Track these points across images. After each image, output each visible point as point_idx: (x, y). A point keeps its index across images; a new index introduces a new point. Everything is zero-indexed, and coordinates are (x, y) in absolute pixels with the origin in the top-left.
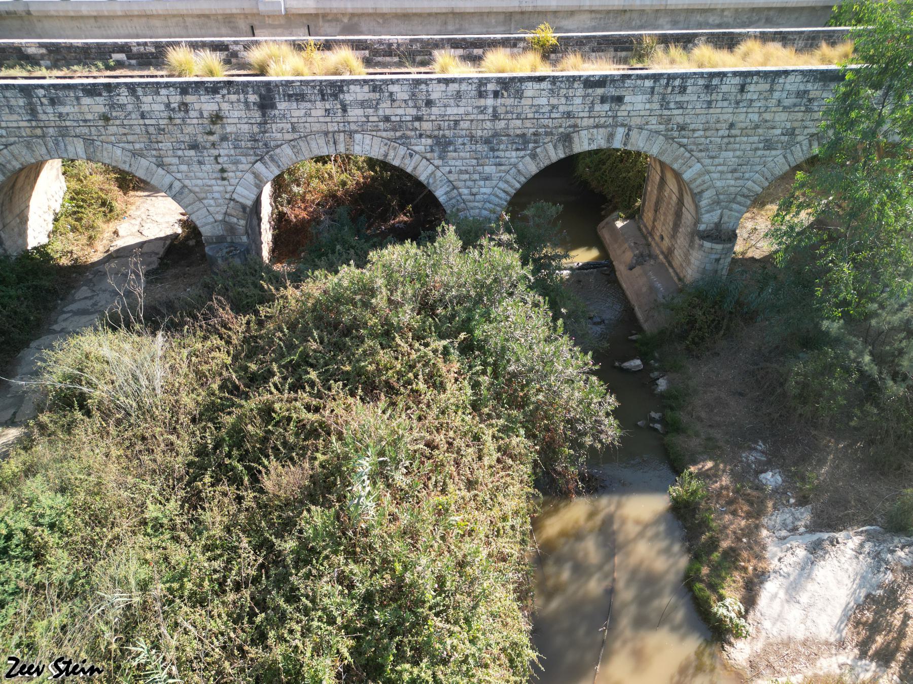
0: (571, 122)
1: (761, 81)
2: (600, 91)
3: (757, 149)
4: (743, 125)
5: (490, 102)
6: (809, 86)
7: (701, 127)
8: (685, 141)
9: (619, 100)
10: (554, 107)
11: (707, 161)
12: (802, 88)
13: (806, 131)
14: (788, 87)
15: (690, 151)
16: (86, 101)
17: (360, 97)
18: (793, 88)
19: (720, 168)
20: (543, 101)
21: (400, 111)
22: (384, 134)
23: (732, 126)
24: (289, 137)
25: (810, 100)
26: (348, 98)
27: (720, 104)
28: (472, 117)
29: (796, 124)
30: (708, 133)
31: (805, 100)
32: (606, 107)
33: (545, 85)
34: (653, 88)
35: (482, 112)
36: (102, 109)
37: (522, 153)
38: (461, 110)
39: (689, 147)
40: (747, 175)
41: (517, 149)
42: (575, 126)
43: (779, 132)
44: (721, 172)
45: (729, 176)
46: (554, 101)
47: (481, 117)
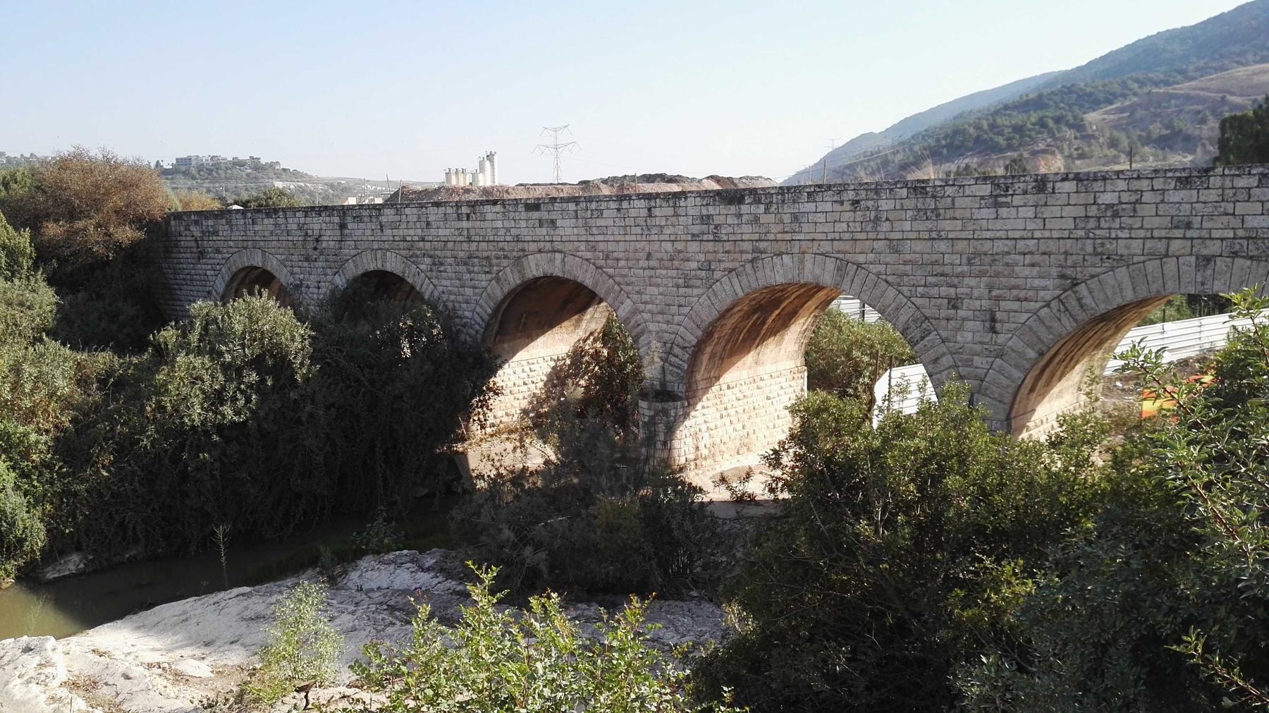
0: (520, 245)
1: (664, 204)
2: (536, 215)
3: (678, 287)
4: (659, 255)
5: (465, 224)
6: (711, 210)
7: (621, 255)
8: (611, 271)
9: (553, 222)
10: (508, 230)
11: (636, 297)
12: (704, 212)
13: (723, 266)
15: (619, 284)
16: (266, 221)
19: (649, 307)
20: (499, 224)
21: (412, 232)
22: (403, 252)
23: (649, 257)
26: (383, 219)
28: (454, 238)
29: (710, 257)
30: (631, 264)
31: (712, 227)
32: (544, 231)
33: (498, 208)
34: (576, 211)
35: (460, 235)
36: (271, 228)
37: (489, 276)
38: (447, 232)
39: (617, 279)
40: (677, 319)
41: (486, 273)
42: (523, 250)
43: (694, 265)
44: (652, 313)
45: (659, 318)
46: (507, 224)
47: (460, 238)
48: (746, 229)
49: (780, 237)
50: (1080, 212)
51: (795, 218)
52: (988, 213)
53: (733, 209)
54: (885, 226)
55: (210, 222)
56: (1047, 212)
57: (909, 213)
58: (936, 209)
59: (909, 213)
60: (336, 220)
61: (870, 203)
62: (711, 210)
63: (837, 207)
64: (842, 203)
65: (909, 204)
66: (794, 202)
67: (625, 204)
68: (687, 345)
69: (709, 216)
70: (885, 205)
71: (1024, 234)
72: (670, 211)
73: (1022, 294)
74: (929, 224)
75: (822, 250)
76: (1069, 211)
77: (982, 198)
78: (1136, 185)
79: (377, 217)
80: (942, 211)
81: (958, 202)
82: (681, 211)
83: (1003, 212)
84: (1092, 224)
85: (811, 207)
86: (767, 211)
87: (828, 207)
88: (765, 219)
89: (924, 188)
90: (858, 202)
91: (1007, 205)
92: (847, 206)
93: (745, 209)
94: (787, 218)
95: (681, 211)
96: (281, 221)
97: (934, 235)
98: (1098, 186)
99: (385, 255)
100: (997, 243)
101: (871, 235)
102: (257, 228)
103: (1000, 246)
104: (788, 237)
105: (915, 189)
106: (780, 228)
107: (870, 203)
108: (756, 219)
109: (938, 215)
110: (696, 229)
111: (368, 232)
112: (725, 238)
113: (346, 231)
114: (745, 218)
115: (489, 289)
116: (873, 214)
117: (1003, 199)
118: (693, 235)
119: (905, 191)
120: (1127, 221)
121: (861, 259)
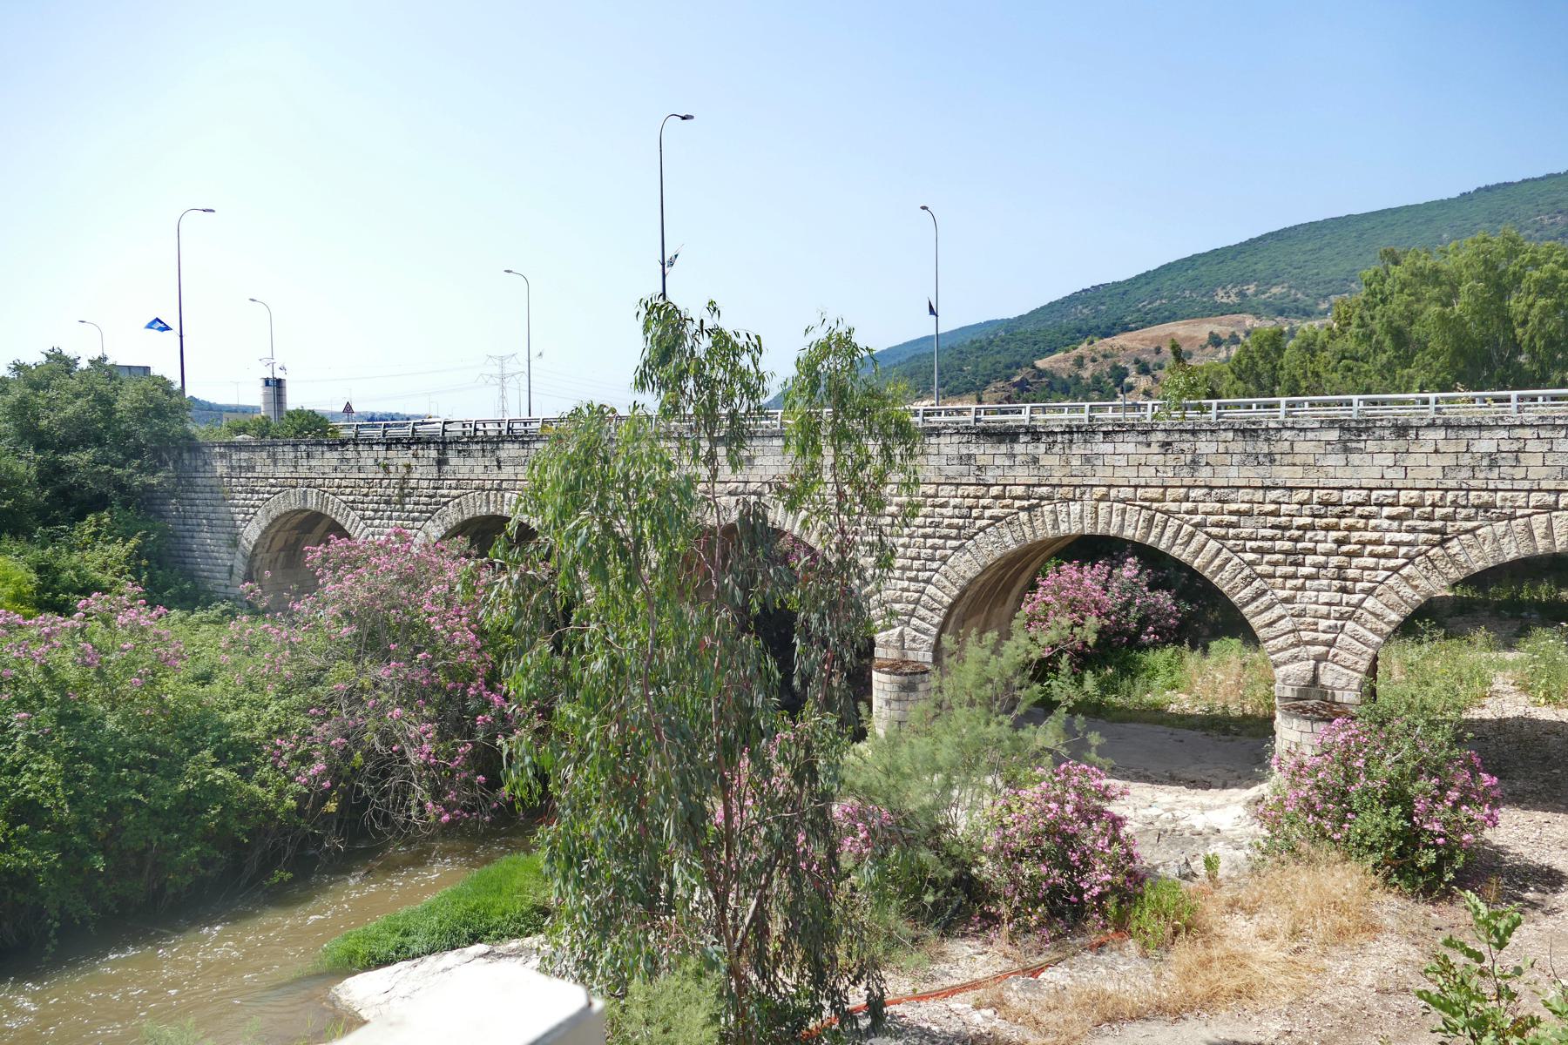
6: (973, 450)
12: (964, 451)
14: (946, 450)
16: (328, 455)
17: (513, 453)
18: (952, 451)
24: (454, 492)
25: (979, 468)
26: (502, 454)
36: (335, 463)
49: (1065, 481)
50: (1449, 460)
51: (1087, 459)
52: (1339, 459)
53: (1003, 448)
54: (1204, 474)
55: (244, 455)
56: (1410, 461)
57: (1236, 458)
58: (1270, 454)
59: (1236, 458)
60: (433, 454)
61: (1185, 446)
62: (973, 450)
63: (1145, 450)
64: (1149, 445)
65: (1238, 446)
66: (1086, 441)
68: (936, 605)
69: (969, 456)
71: (1382, 483)
73: (1379, 549)
74: (1261, 470)
75: (1122, 496)
76: (1435, 460)
77: (1328, 443)
78: (1519, 433)
79: (493, 451)
80: (1278, 457)
81: (1298, 447)
83: (1355, 458)
84: (1465, 473)
85: (1108, 448)
86: (1048, 451)
87: (1130, 448)
88: (1046, 460)
89: (1255, 431)
90: (1169, 444)
91: (1361, 451)
92: (1155, 448)
93: (1019, 448)
94: (1076, 462)
96: (349, 455)
97: (1268, 483)
98: (1474, 434)
100: (1346, 493)
101: (1188, 482)
102: (313, 463)
103: (1350, 496)
104: (1076, 481)
105: (1243, 431)
106: (1067, 470)
107: (1185, 446)
108: (1035, 460)
109: (1272, 461)
110: (952, 470)
111: (479, 470)
112: (992, 481)
113: (446, 468)
114: (1019, 459)
116: (1189, 457)
117: (1354, 445)
118: (947, 477)
119: (1230, 435)
120: (1506, 471)
121: (1173, 507)
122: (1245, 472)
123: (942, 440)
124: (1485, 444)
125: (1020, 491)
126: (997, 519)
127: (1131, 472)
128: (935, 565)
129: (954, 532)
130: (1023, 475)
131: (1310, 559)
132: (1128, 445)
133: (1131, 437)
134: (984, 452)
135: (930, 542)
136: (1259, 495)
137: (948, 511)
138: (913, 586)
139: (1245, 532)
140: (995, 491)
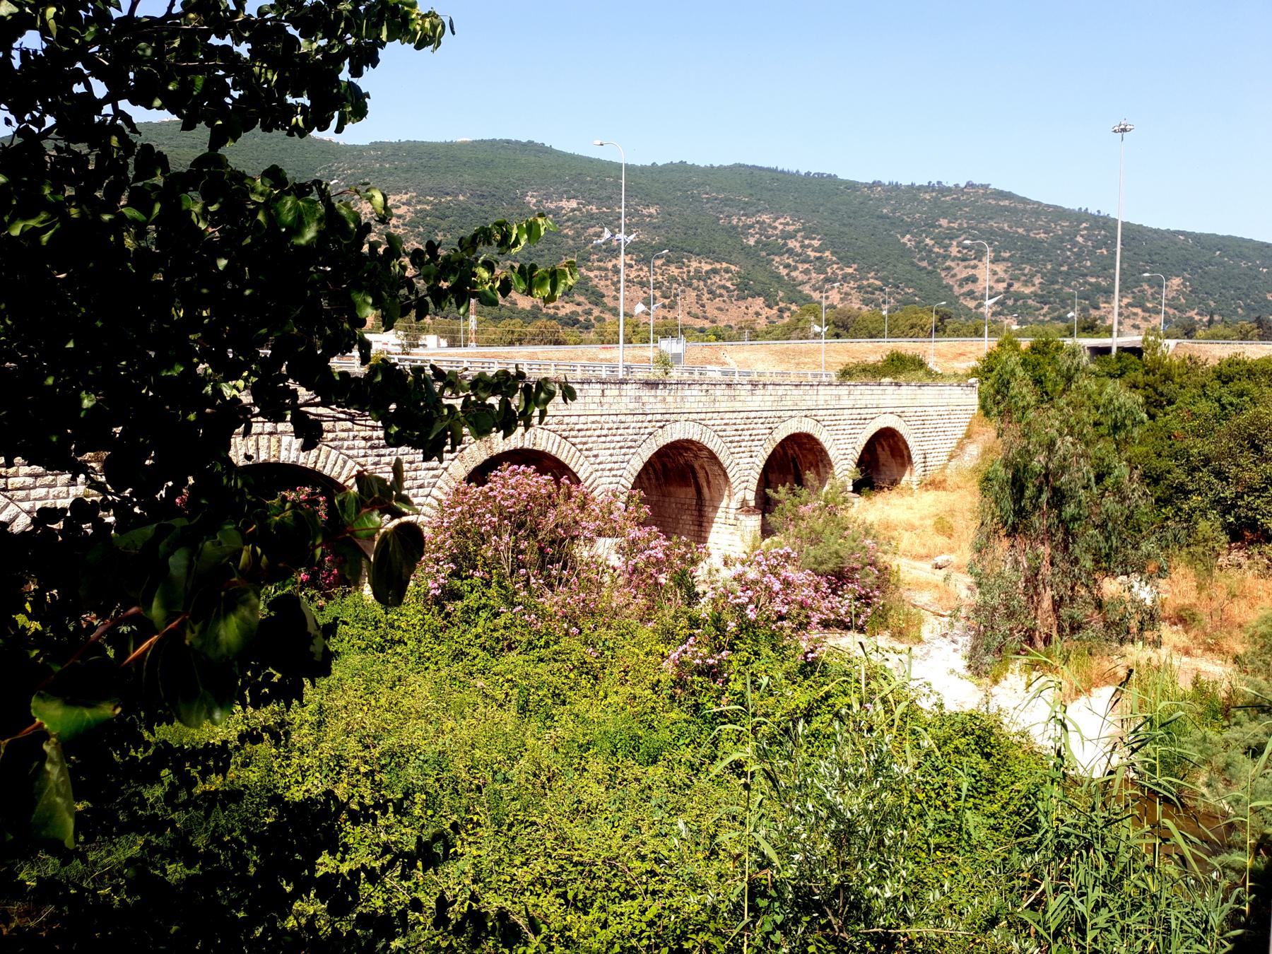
6: (641, 393)
14: (629, 393)
27: (592, 406)
48: (659, 405)
52: (749, 398)
53: (653, 392)
54: (717, 404)
65: (726, 392)
67: (586, 386)
70: (718, 393)
72: (616, 392)
82: (623, 393)
85: (688, 393)
87: (695, 393)
88: (669, 399)
93: (659, 392)
95: (623, 393)
99: (279, 441)
110: (631, 406)
115: (450, 470)
122: (729, 404)
123: (629, 386)
124: (780, 393)
125: (659, 417)
126: (650, 434)
127: (695, 405)
128: (624, 465)
129: (633, 444)
130: (660, 408)
131: (743, 444)
132: (695, 390)
133: (697, 387)
134: (646, 394)
135: (623, 451)
136: (731, 415)
137: (630, 431)
138: (615, 480)
139: (727, 433)
140: (649, 417)
